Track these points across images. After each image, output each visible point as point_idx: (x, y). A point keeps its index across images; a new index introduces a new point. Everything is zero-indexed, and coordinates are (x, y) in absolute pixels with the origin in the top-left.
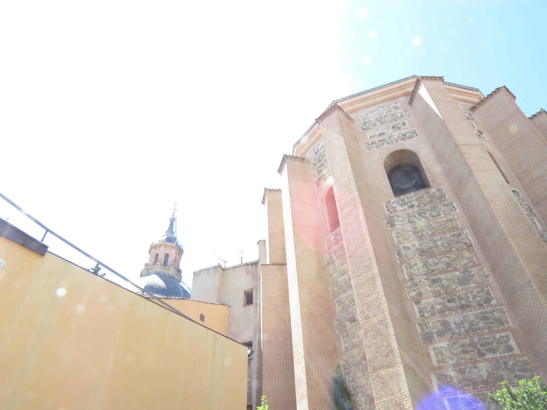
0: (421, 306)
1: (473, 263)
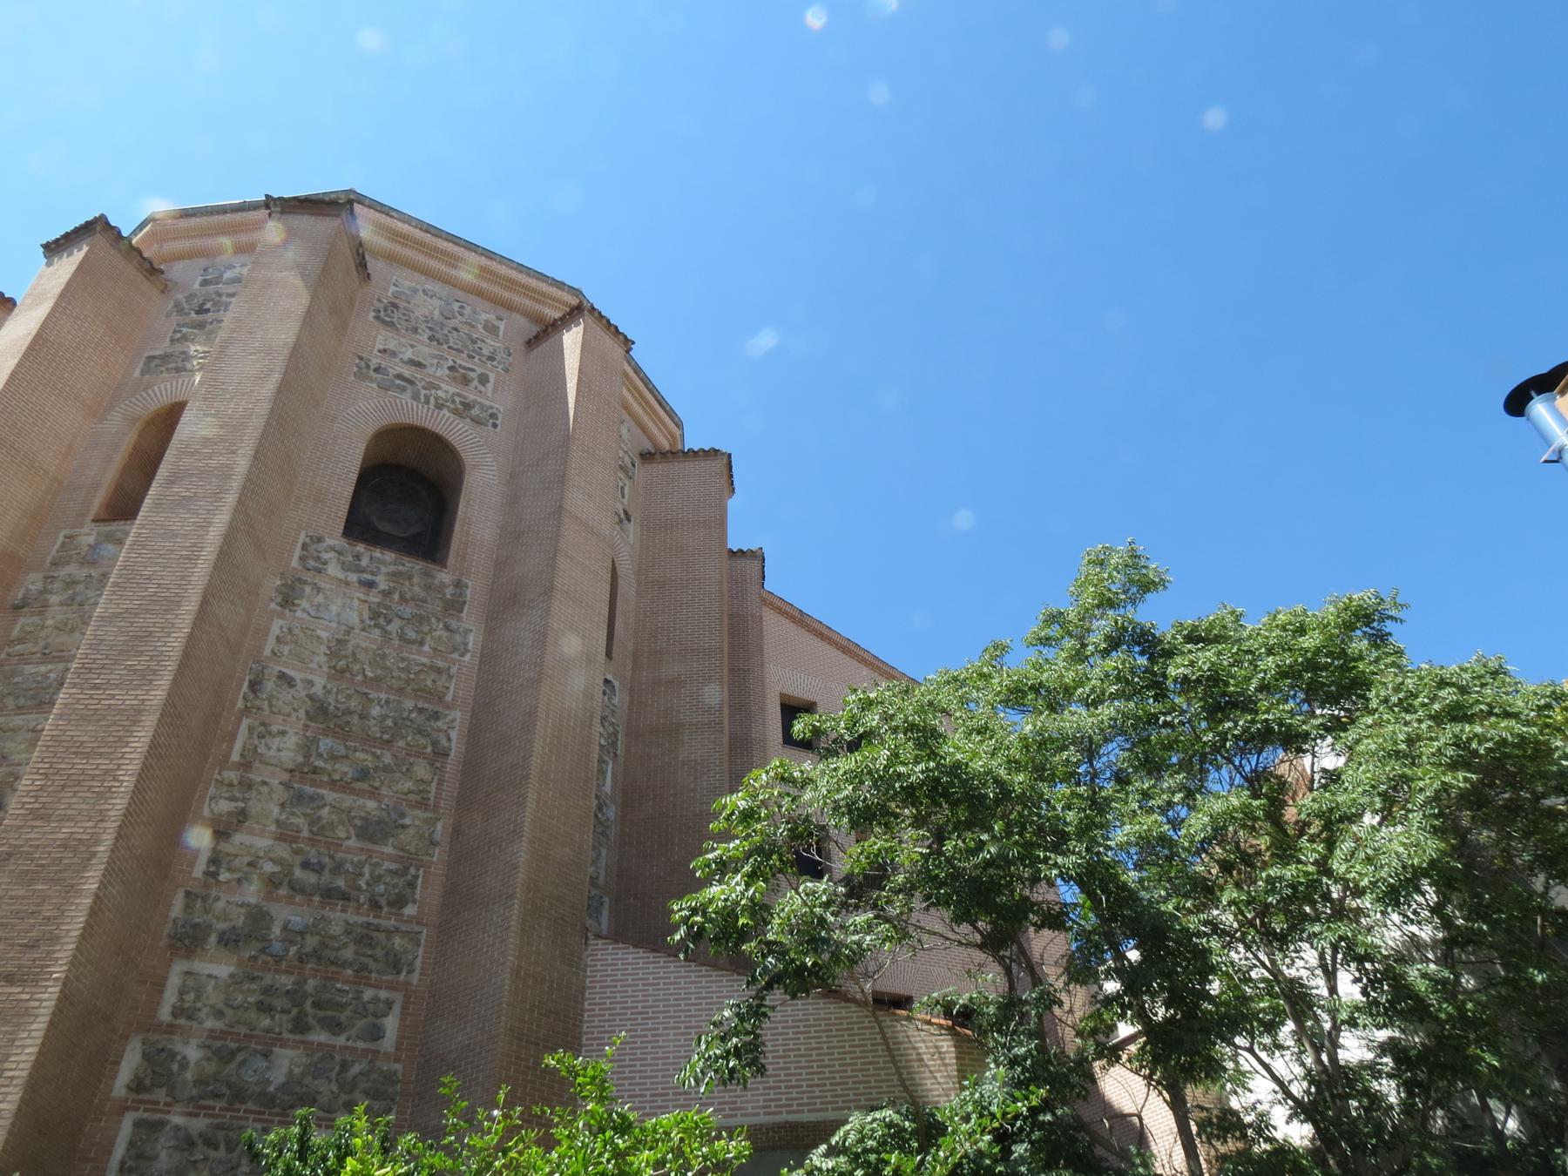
0: (225, 847)
1: (423, 798)
